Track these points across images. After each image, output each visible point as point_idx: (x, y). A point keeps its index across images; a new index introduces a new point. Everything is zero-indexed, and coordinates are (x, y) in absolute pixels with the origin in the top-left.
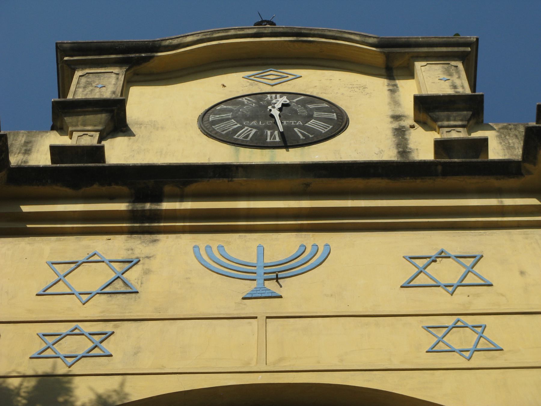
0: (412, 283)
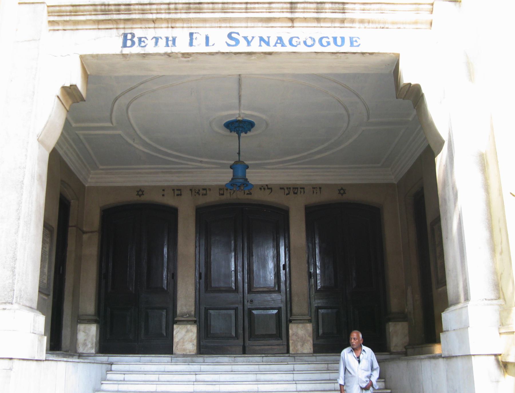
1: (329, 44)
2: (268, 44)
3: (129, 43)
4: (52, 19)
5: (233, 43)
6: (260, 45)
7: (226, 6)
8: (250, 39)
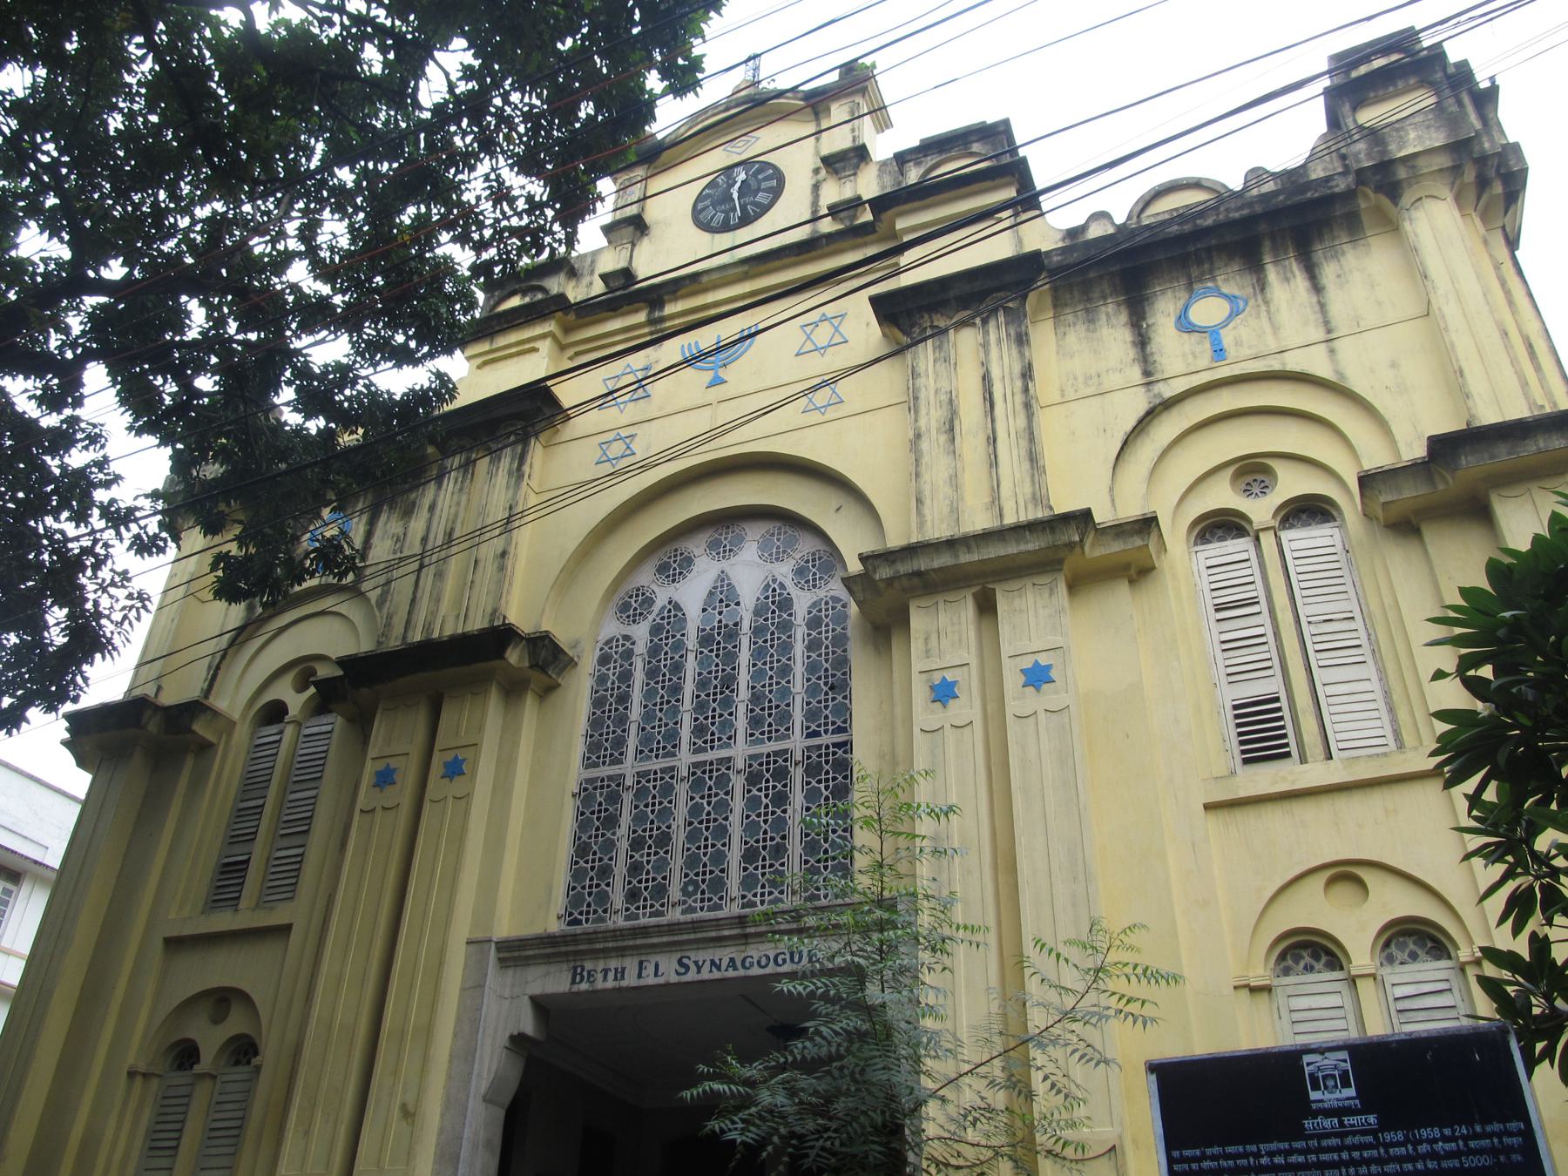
0: (802, 351)
1: (784, 961)
2: (719, 968)
3: (578, 977)
4: (501, 955)
5: (683, 970)
6: (711, 971)
7: (672, 928)
8: (700, 963)
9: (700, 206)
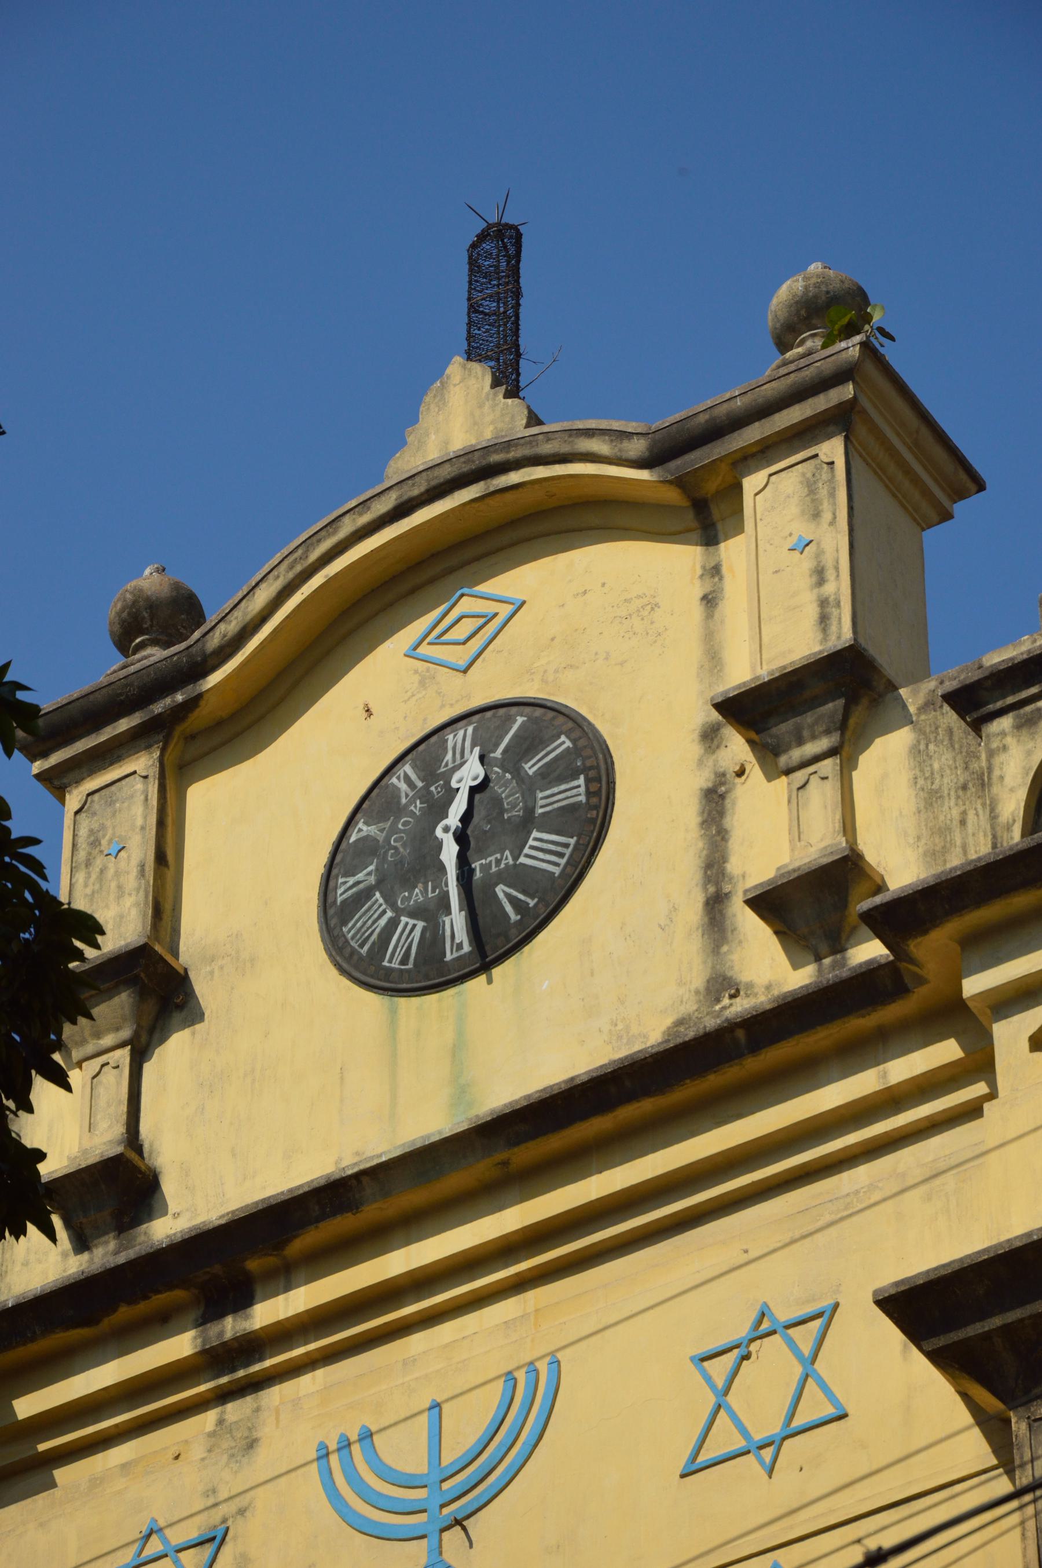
0: (703, 1458)
9: (344, 888)
